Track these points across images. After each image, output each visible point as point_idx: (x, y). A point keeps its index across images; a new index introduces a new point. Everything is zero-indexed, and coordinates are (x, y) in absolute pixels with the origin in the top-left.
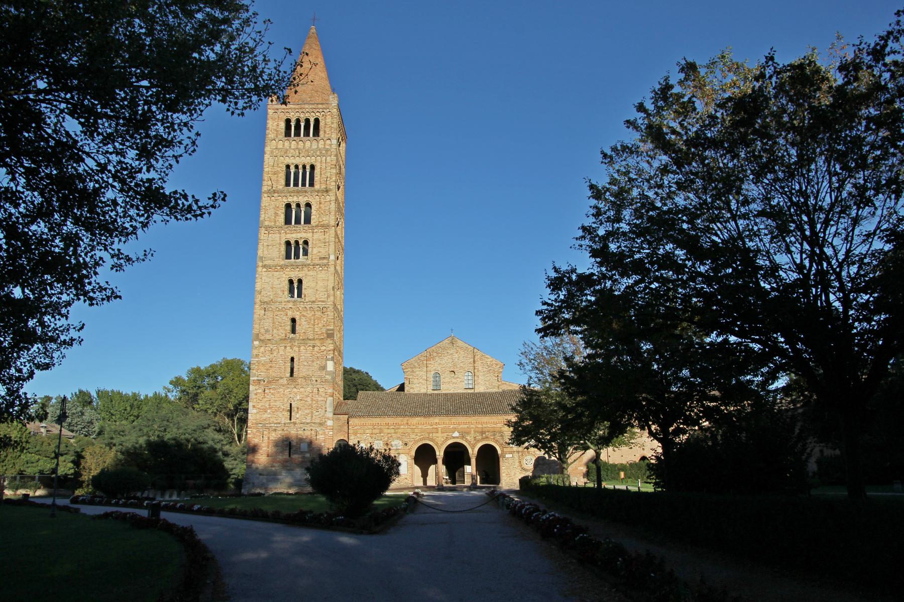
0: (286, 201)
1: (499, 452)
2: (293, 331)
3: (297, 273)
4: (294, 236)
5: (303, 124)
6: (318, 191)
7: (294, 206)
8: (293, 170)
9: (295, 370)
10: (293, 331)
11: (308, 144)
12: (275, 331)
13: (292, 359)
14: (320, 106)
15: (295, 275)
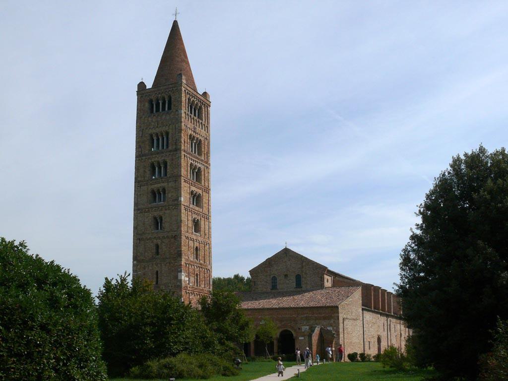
0: (150, 161)
1: (294, 335)
2: (157, 253)
3: (158, 212)
4: (156, 185)
5: (161, 102)
6: (170, 151)
7: (156, 164)
8: (155, 138)
9: (159, 279)
10: (157, 253)
11: (164, 117)
12: (146, 254)
13: (157, 272)
14: (170, 86)
15: (156, 214)
